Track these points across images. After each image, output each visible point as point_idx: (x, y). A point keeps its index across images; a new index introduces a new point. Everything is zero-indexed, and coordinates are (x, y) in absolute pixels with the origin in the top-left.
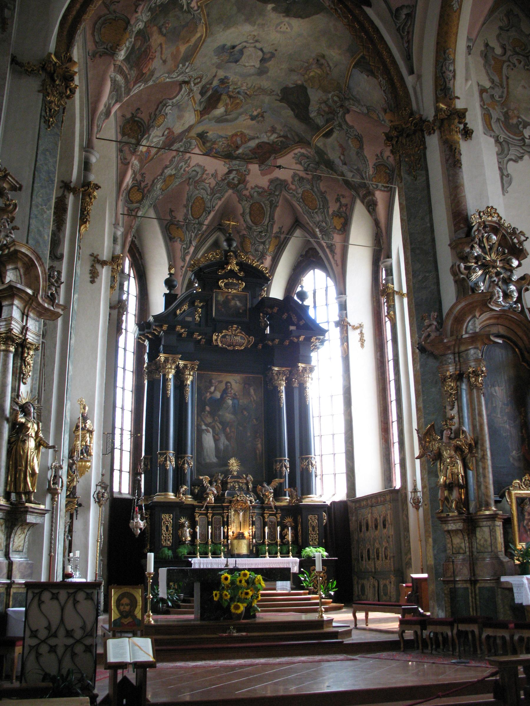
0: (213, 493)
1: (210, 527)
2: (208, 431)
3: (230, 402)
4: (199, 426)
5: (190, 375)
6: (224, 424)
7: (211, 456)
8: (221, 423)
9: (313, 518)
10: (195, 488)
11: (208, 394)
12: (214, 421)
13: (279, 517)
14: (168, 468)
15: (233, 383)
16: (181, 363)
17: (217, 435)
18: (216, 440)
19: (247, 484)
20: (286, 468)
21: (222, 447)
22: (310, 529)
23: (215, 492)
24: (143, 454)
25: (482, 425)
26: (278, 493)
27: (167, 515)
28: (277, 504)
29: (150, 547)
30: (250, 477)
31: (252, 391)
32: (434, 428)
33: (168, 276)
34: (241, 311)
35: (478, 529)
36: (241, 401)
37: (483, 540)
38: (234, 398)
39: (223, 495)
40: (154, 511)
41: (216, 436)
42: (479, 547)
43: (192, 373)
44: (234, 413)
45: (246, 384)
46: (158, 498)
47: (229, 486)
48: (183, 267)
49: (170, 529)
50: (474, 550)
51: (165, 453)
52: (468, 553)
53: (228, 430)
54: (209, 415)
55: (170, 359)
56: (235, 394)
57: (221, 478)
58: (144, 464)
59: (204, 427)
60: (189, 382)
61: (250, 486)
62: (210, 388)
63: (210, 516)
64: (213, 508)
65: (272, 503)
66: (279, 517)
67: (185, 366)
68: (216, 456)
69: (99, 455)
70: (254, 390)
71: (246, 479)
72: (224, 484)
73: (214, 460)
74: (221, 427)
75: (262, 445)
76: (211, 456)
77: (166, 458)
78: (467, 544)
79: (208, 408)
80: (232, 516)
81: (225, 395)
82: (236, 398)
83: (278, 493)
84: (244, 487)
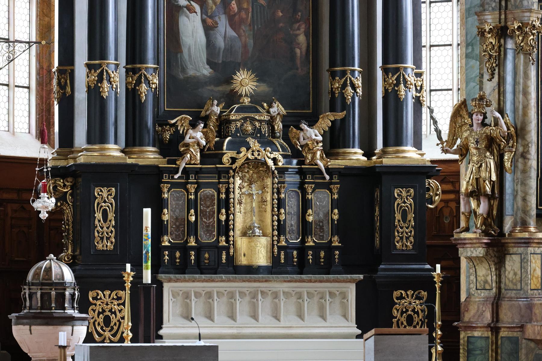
0: (198, 144)
1: (192, 211)
2: (191, 10)
9: (404, 194)
10: (164, 131)
13: (335, 191)
14: (105, 95)
17: (211, 17)
19: (271, 123)
20: (354, 87)
21: (220, 43)
22: (398, 216)
23: (203, 142)
24: (56, 64)
25: (526, 107)
26: (336, 140)
27: (105, 191)
28: (335, 163)
29: (74, 251)
30: (277, 109)
32: (466, 106)
35: (508, 258)
37: (512, 273)
39: (219, 145)
40: (79, 180)
41: (209, 21)
42: (507, 282)
46: (85, 153)
47: (233, 128)
49: (111, 216)
50: (503, 286)
51: (100, 65)
52: (494, 290)
57: (217, 110)
58: (59, 84)
63: (192, 188)
64: (198, 172)
65: (321, 164)
66: (335, 191)
68: (209, 63)
71: (268, 112)
72: (223, 124)
73: (206, 71)
75: (306, 35)
77: (102, 73)
78: (494, 277)
80: (237, 191)
83: (336, 140)
84: (265, 129)
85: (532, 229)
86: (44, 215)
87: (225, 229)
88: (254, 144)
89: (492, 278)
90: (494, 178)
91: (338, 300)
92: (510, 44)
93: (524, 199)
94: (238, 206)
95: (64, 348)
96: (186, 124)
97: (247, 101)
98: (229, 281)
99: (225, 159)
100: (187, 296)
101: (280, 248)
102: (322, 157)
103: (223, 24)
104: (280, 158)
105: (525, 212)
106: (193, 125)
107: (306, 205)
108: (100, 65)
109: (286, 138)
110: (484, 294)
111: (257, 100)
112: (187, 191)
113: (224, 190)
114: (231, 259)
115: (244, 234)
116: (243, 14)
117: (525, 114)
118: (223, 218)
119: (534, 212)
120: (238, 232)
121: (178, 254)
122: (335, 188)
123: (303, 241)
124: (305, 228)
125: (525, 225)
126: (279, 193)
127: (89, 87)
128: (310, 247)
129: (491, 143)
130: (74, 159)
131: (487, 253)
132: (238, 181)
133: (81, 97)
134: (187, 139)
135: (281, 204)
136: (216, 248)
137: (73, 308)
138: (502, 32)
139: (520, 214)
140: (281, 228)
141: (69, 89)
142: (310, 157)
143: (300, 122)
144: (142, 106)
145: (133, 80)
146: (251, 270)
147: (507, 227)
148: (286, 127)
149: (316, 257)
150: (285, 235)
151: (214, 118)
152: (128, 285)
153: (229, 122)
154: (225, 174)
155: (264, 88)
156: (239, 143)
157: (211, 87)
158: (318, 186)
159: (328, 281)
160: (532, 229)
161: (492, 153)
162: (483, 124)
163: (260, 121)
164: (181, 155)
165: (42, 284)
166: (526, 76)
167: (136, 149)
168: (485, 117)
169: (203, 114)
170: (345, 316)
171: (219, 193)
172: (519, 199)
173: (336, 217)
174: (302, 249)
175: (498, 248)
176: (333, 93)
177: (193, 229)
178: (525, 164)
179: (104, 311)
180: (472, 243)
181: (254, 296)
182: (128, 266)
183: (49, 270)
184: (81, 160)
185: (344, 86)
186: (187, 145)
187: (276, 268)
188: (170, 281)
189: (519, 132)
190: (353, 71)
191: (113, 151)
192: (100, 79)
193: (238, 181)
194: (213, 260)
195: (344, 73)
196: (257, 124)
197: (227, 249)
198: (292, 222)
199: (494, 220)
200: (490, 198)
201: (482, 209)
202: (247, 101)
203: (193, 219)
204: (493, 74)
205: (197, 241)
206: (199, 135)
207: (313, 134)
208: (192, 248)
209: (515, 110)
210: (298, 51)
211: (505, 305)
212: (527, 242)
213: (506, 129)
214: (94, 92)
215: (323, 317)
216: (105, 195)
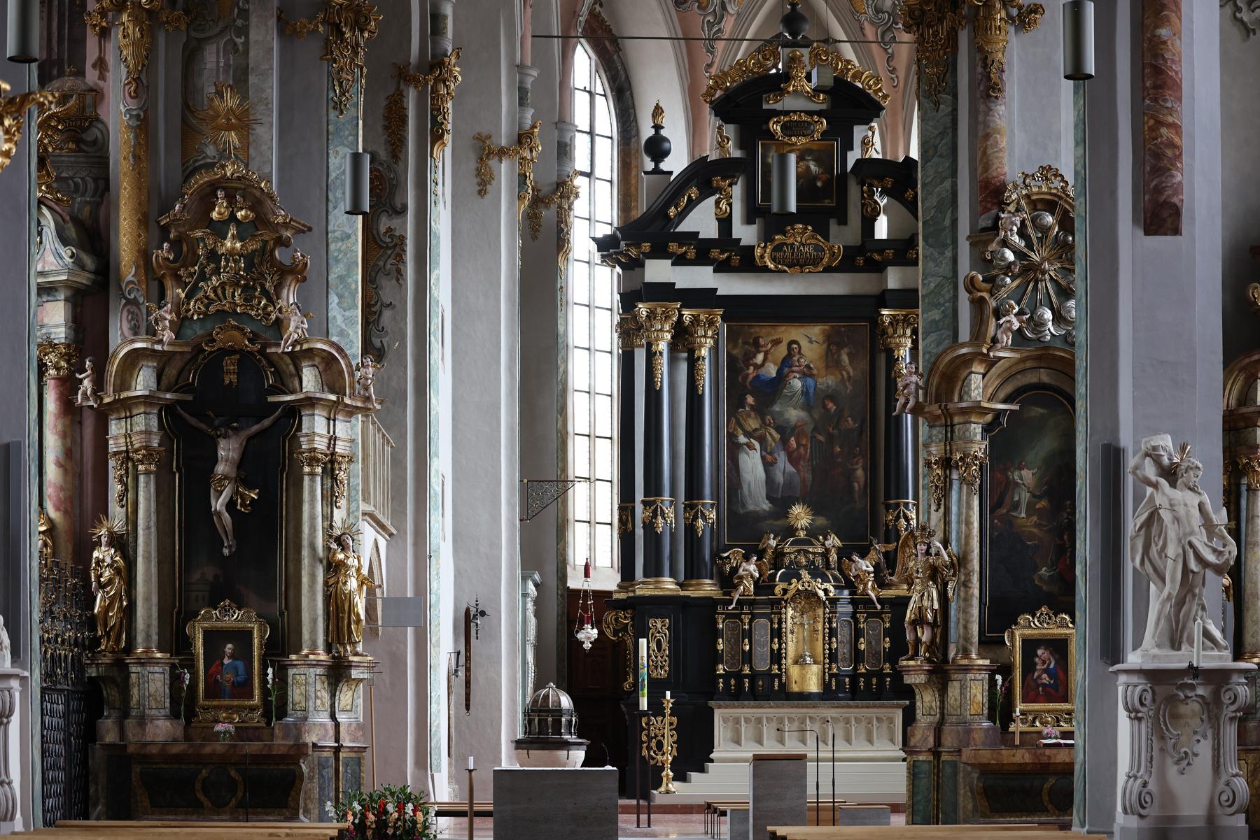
0: (752, 576)
2: (751, 447)
3: (797, 384)
4: (732, 436)
5: (705, 336)
6: (785, 431)
7: (757, 498)
8: (777, 429)
11: (752, 368)
12: (764, 424)
15: (804, 343)
16: (687, 313)
17: (771, 453)
18: (768, 465)
19: (825, 555)
21: (780, 478)
23: (757, 575)
25: (968, 536)
28: (886, 593)
30: (833, 541)
31: (845, 358)
33: (653, 132)
34: (819, 184)
36: (820, 380)
38: (807, 373)
41: (769, 458)
43: (710, 333)
44: (807, 407)
45: (833, 343)
47: (787, 561)
48: (710, 66)
49: (665, 645)
51: (655, 502)
53: (793, 441)
54: (753, 414)
55: (659, 310)
56: (808, 366)
57: (773, 543)
59: (742, 439)
60: (704, 352)
61: (834, 557)
62: (755, 356)
64: (752, 603)
65: (873, 595)
67: (696, 320)
69: (514, 525)
70: (848, 354)
71: (823, 545)
72: (779, 555)
73: (766, 506)
74: (777, 436)
75: (865, 470)
76: (757, 498)
79: (750, 400)
80: (789, 621)
81: (786, 370)
82: (811, 376)
84: (819, 561)
85: (974, 656)
86: (587, 646)
87: (777, 657)
88: (805, 575)
89: (936, 704)
90: (936, 606)
91: (885, 725)
92: (955, 476)
93: (965, 627)
94: (790, 636)
95: (470, 771)
96: (739, 557)
97: (802, 534)
98: (778, 707)
99: (778, 590)
100: (737, 721)
101: (831, 676)
102: (873, 588)
103: (782, 461)
104: (832, 589)
105: (967, 639)
106: (747, 558)
107: (858, 633)
108: (655, 502)
109: (841, 570)
110: (929, 719)
111: (813, 532)
112: (742, 620)
113: (776, 620)
114: (783, 686)
115: (796, 662)
116: (802, 450)
117: (967, 543)
118: (776, 647)
119: (976, 639)
120: (790, 661)
121: (733, 682)
122: (887, 617)
123: (855, 669)
124: (858, 657)
125: (966, 653)
126: (830, 622)
127: (644, 523)
128: (862, 675)
129: (934, 573)
130: (634, 591)
131: (929, 681)
132: (790, 612)
133: (639, 532)
134: (741, 572)
135: (832, 632)
136: (769, 676)
137: (570, 733)
138: (947, 463)
139: (961, 641)
140: (833, 657)
141: (630, 525)
142: (861, 587)
143: (851, 554)
144: (700, 540)
145: (690, 515)
146: (803, 697)
147: (951, 655)
148: (840, 558)
149: (868, 684)
150: (836, 662)
151: (770, 551)
152: (668, 711)
153: (784, 554)
154: (777, 605)
155: (821, 521)
156: (792, 574)
157: (771, 522)
158: (870, 615)
159: (874, 707)
160: (974, 656)
161: (935, 582)
162: (928, 553)
163: (814, 553)
164: (736, 587)
165: (540, 711)
166: (969, 507)
167: (694, 582)
168: (929, 547)
169: (761, 547)
170: (892, 741)
171: (772, 623)
172: (961, 627)
173: (887, 646)
174: (854, 677)
175: (941, 674)
176: (887, 525)
177: (748, 657)
178: (967, 593)
179: (656, 736)
180: (916, 670)
181: (803, 722)
182: (668, 693)
183: (546, 697)
184: (638, 593)
185: (898, 518)
186: (741, 578)
187: (828, 694)
188: (720, 707)
189: (960, 562)
190: (906, 505)
191: (668, 585)
192: (655, 515)
193: (790, 612)
194: (768, 688)
195: (898, 505)
196: (811, 556)
197: (779, 676)
198: (844, 651)
199: (939, 647)
200: (933, 626)
201: (925, 635)
202: (802, 534)
203: (747, 648)
204: (939, 505)
205: (751, 669)
206: (752, 568)
207: (865, 565)
208: (746, 676)
209: (958, 540)
210: (856, 485)
211: (947, 729)
212: (967, 669)
213: (947, 558)
214: (649, 527)
215: (870, 741)
216: (659, 626)
